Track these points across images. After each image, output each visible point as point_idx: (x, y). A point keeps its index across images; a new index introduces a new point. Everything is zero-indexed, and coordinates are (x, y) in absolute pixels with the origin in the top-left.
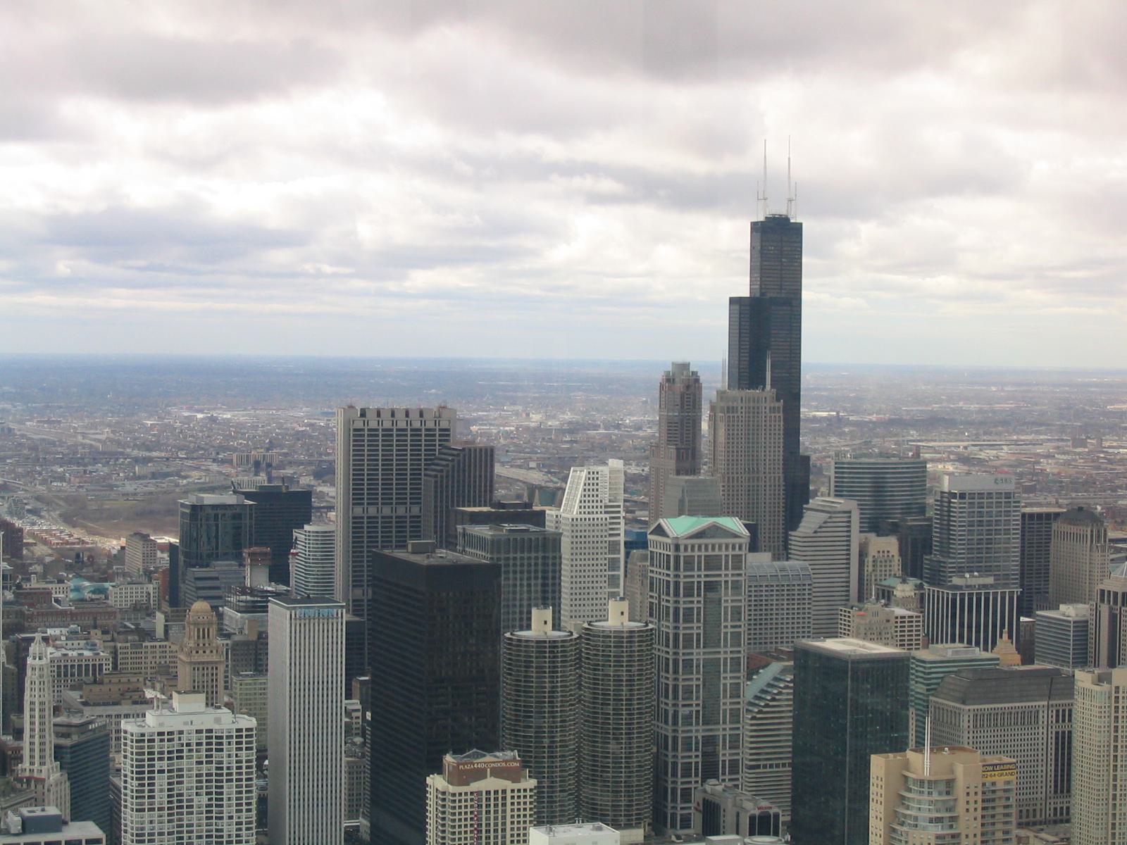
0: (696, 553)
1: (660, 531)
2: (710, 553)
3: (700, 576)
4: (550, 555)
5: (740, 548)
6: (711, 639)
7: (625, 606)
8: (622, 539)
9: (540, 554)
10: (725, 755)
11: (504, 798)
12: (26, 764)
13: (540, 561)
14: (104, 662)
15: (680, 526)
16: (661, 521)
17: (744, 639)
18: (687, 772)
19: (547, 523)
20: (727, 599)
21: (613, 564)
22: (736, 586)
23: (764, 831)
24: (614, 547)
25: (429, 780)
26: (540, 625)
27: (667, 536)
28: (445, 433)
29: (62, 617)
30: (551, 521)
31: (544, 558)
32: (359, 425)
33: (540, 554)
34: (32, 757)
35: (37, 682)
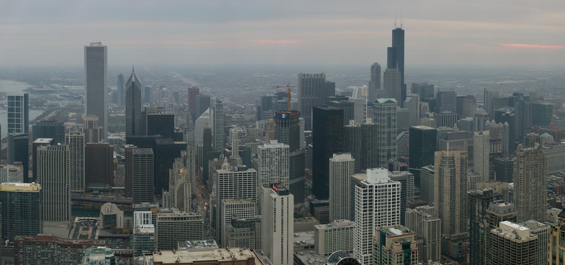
1: (377, 102)
3: (386, 112)
6: (389, 126)
7: (370, 119)
10: (392, 153)
12: (232, 155)
15: (381, 101)
17: (396, 126)
20: (393, 118)
21: (365, 110)
23: (404, 170)
24: (365, 106)
26: (352, 124)
28: (323, 79)
29: (234, 123)
32: (303, 78)
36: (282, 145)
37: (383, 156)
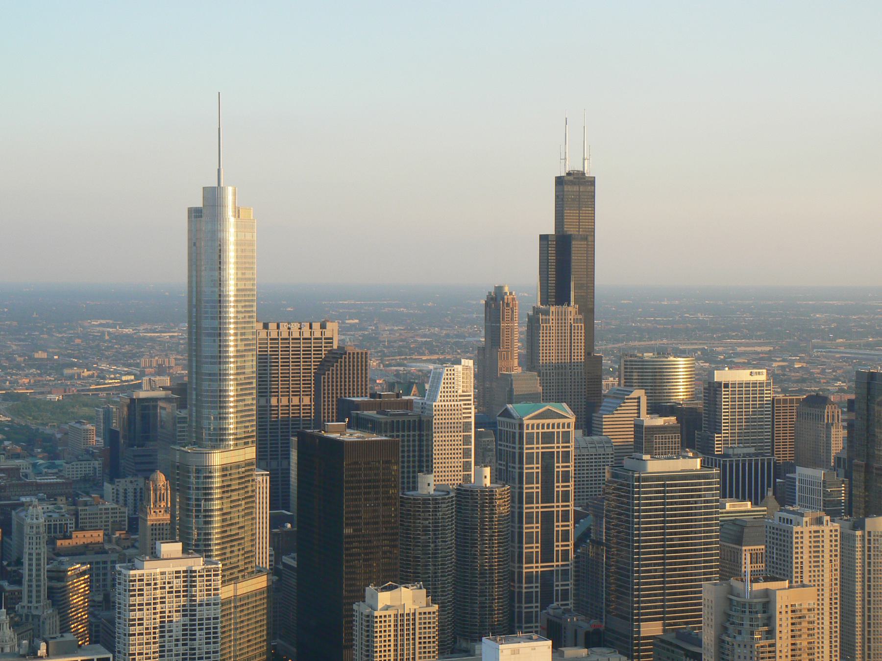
0: (535, 431)
2: (546, 430)
3: (537, 448)
4: (424, 433)
5: (569, 427)
6: (547, 495)
8: (473, 420)
9: (417, 433)
11: (414, 619)
12: (25, 602)
13: (417, 438)
14: (69, 522)
16: (509, 406)
18: (529, 599)
19: (415, 409)
21: (466, 441)
22: (566, 456)
24: (467, 426)
25: (355, 607)
27: (514, 418)
30: (417, 408)
31: (420, 435)
32: (263, 334)
33: (417, 433)
34: (30, 597)
35: (34, 538)
36: (197, 563)
37: (529, 598)
